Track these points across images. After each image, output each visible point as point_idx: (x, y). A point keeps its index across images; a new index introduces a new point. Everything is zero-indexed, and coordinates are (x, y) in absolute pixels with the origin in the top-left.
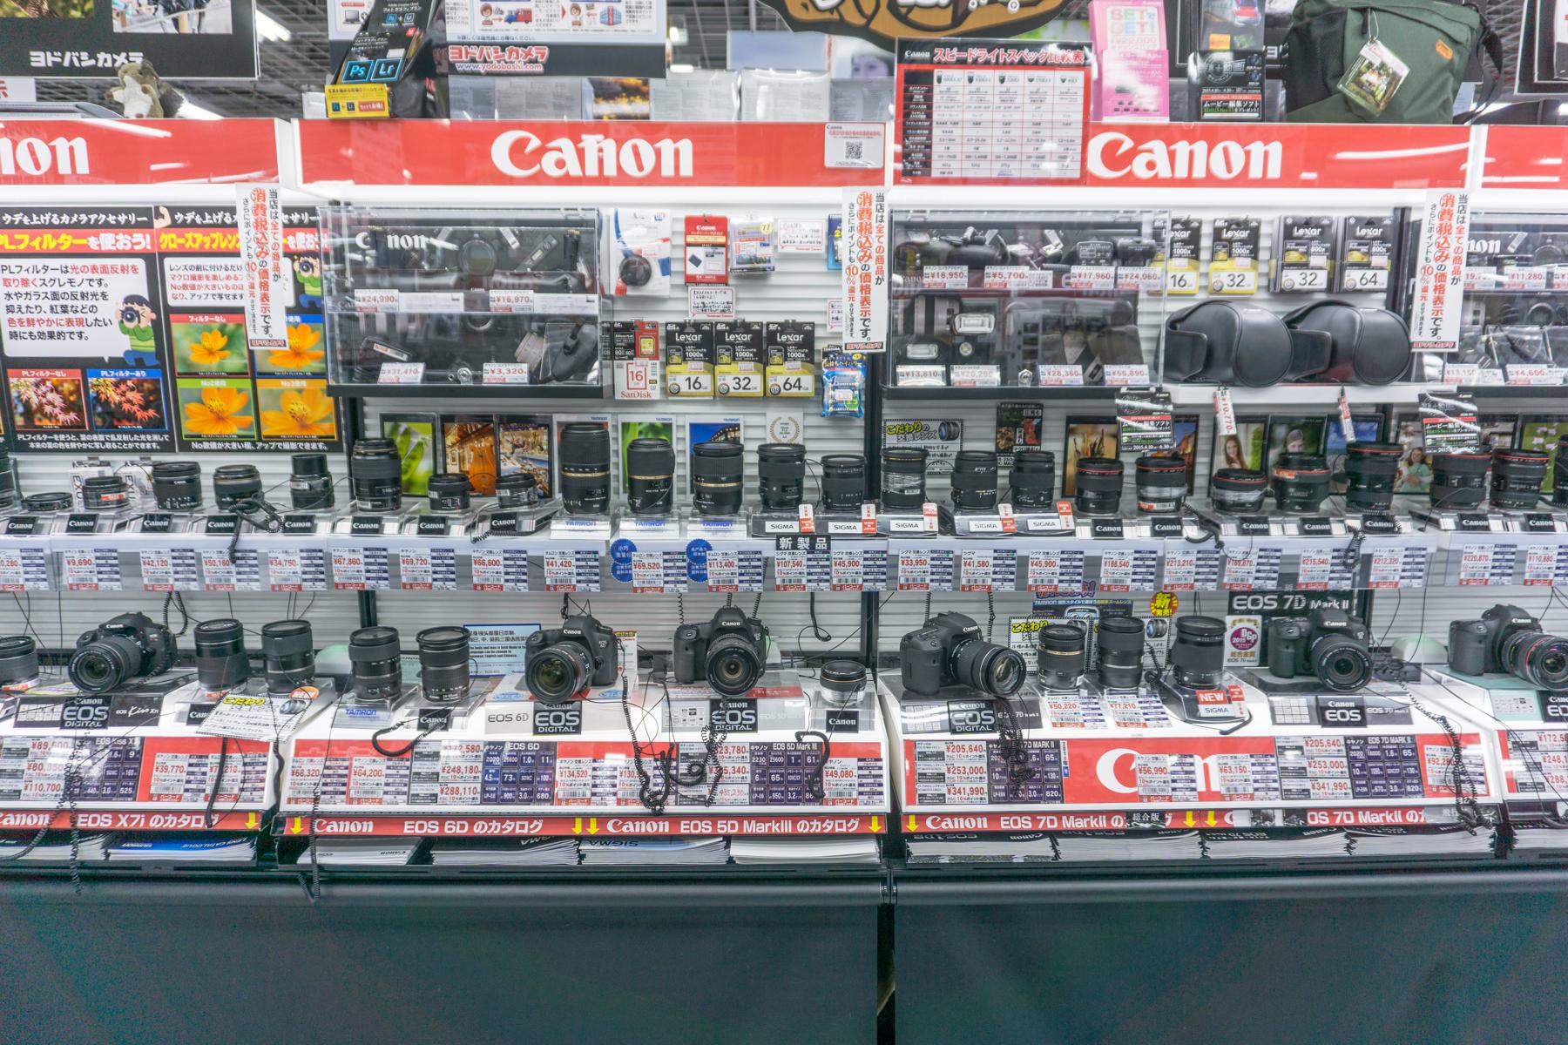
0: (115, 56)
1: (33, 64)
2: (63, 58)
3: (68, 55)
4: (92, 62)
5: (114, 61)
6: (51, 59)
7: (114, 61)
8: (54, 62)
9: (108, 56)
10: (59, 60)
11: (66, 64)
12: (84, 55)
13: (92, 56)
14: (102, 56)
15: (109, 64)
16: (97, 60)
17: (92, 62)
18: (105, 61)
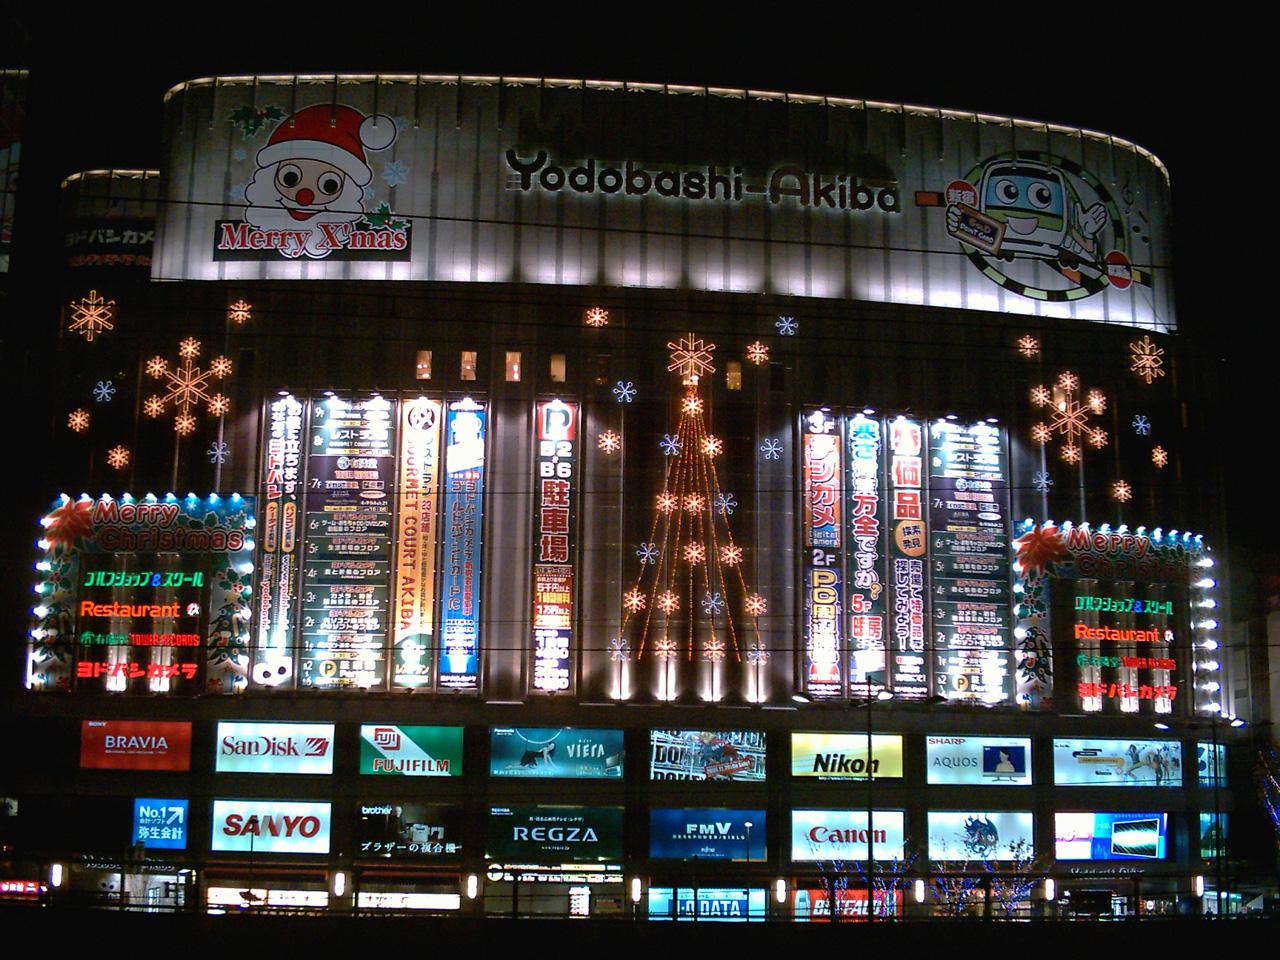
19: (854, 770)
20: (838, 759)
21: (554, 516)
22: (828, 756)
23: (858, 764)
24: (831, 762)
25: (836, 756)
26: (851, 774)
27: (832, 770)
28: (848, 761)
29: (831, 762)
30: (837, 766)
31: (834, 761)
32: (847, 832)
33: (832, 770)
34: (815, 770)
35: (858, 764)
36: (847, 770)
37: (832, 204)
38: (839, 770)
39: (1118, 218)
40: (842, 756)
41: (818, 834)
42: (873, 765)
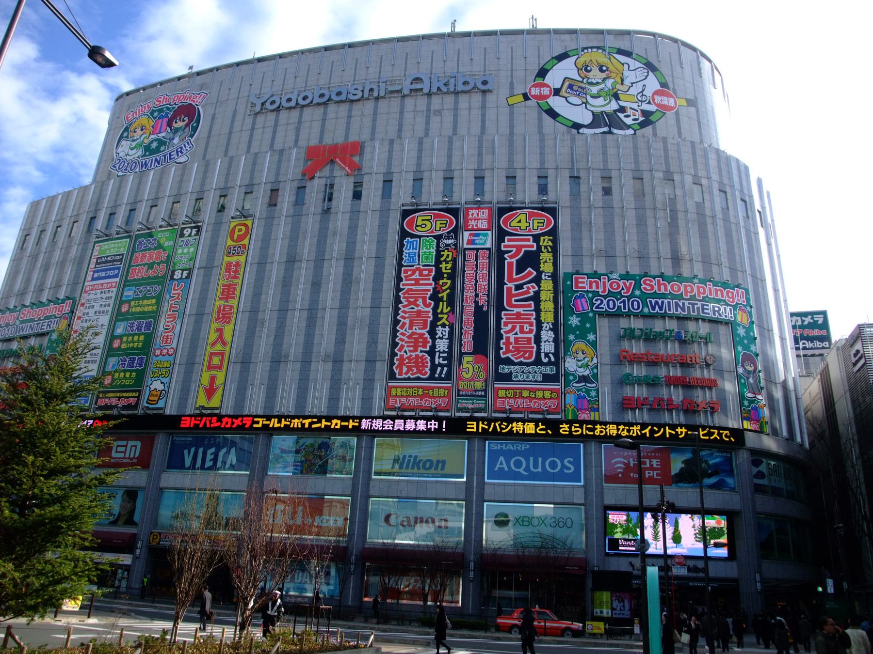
19: (424, 468)
20: (412, 459)
21: (229, 289)
22: (404, 457)
23: (428, 464)
24: (406, 461)
25: (410, 456)
26: (422, 471)
27: (407, 468)
28: (420, 461)
29: (406, 461)
30: (410, 466)
31: (409, 461)
32: (416, 518)
33: (407, 468)
34: (393, 468)
35: (428, 464)
36: (419, 468)
38: (413, 468)
39: (663, 81)
40: (416, 457)
41: (392, 520)
42: (440, 465)
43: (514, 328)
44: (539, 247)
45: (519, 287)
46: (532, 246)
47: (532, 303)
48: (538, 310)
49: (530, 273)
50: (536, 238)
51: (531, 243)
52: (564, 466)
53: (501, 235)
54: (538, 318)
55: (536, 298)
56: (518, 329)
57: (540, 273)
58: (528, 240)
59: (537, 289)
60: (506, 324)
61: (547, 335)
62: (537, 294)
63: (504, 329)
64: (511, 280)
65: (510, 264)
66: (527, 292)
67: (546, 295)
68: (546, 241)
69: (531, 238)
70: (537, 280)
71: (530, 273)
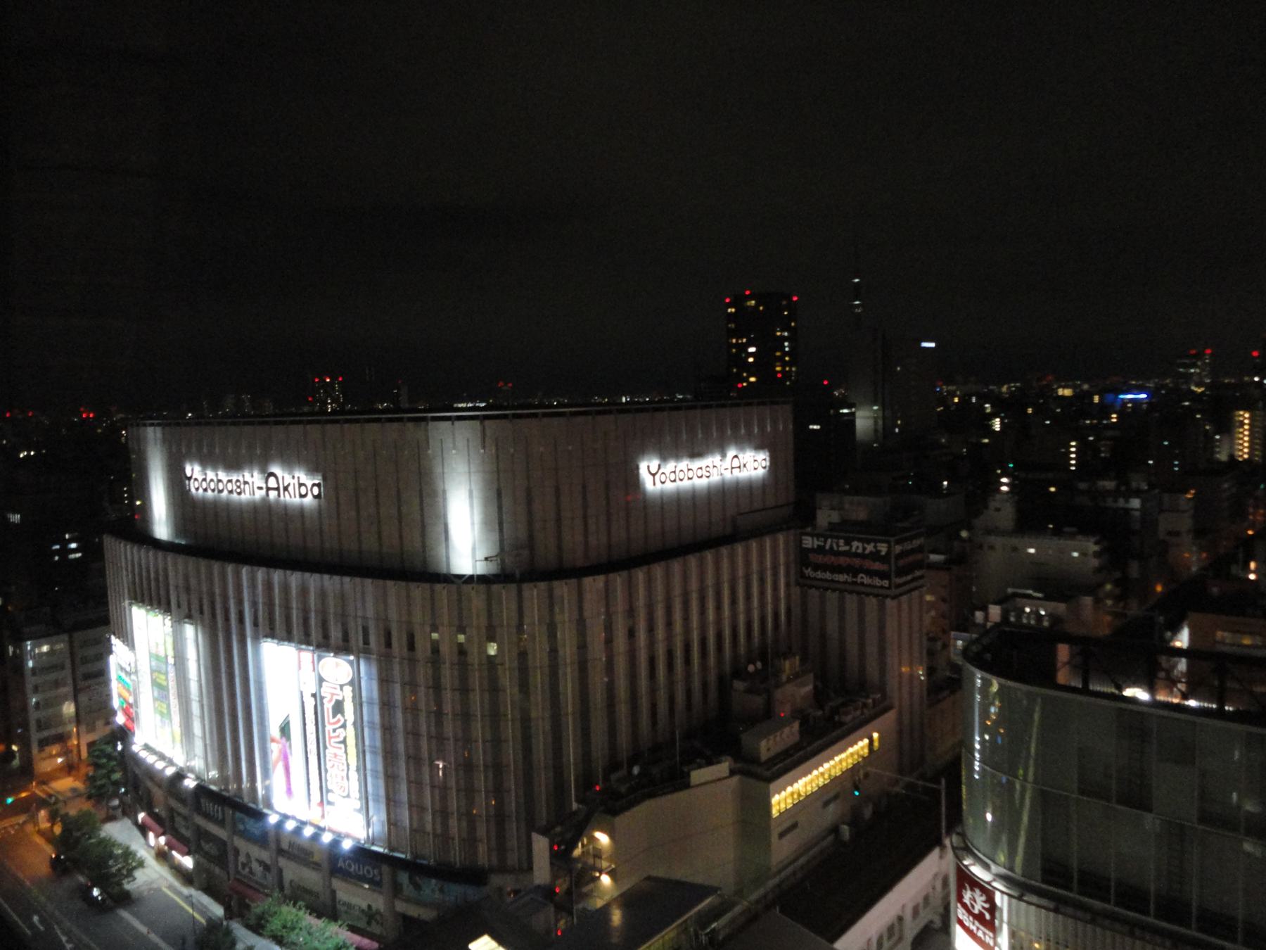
0: (866, 546)
1: (804, 546)
2: (825, 542)
3: (829, 540)
4: (847, 548)
5: (864, 549)
6: (816, 543)
7: (864, 549)
8: (818, 546)
9: (860, 545)
10: (823, 544)
11: (827, 547)
12: (841, 542)
13: (848, 543)
14: (855, 544)
15: (860, 551)
16: (851, 547)
17: (847, 548)
18: (858, 547)
37: (291, 497)
43: (333, 766)
44: (343, 697)
45: (334, 730)
46: (338, 695)
47: (342, 746)
48: (346, 752)
49: (339, 721)
50: (342, 687)
51: (338, 691)
52: (374, 875)
53: (321, 680)
54: (347, 759)
55: (344, 742)
56: (336, 766)
57: (345, 721)
58: (335, 688)
59: (344, 735)
60: (330, 760)
61: (354, 775)
62: (345, 738)
63: (329, 765)
64: (330, 723)
65: (328, 709)
66: (338, 736)
67: (351, 742)
68: (348, 691)
69: (339, 687)
70: (344, 726)
71: (339, 721)
